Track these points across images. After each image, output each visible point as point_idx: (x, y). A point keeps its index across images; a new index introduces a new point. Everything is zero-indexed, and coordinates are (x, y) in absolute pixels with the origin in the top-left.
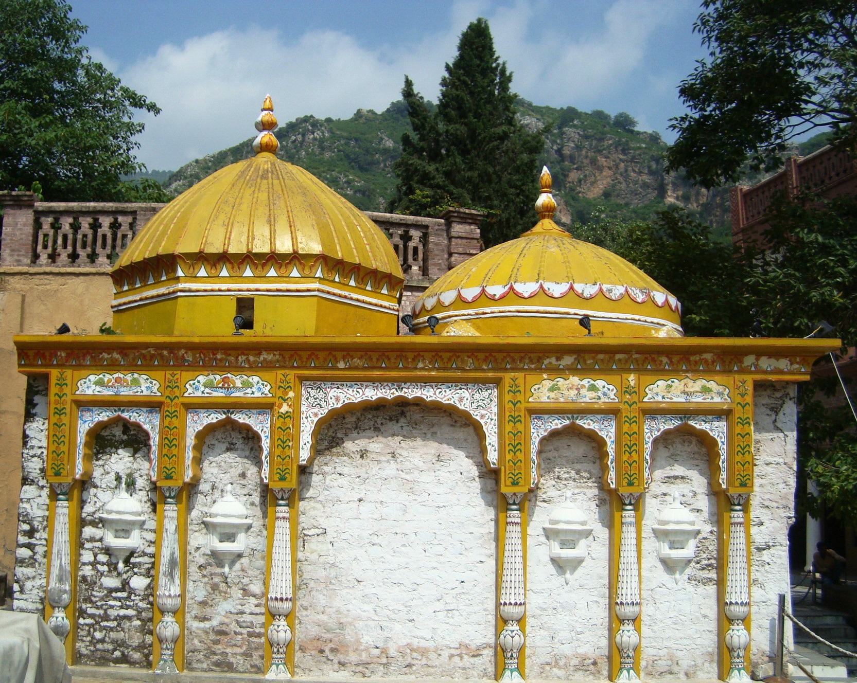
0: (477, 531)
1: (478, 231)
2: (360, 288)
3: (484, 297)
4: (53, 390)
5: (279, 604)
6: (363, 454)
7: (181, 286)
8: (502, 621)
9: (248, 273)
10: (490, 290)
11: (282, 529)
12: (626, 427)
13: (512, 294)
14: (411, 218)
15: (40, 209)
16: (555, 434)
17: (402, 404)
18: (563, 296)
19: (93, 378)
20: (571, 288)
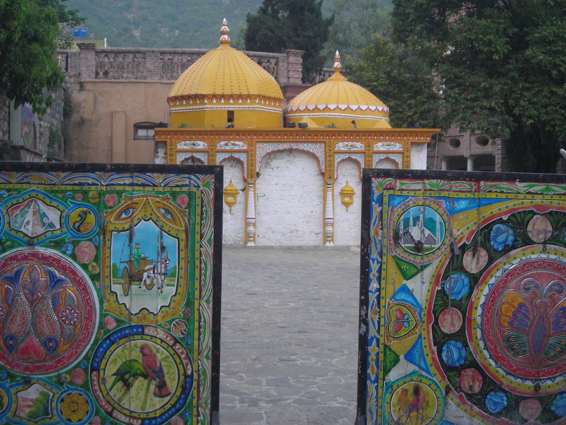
0: (316, 194)
1: (301, 60)
2: (269, 105)
3: (316, 109)
4: (169, 147)
5: (251, 220)
6: (278, 167)
7: (207, 106)
8: (325, 225)
9: (231, 101)
10: (319, 107)
11: (251, 194)
12: (367, 159)
13: (327, 109)
14: (271, 54)
15: (98, 51)
16: (343, 161)
17: (291, 151)
18: (345, 109)
19: (183, 142)
20: (348, 106)
